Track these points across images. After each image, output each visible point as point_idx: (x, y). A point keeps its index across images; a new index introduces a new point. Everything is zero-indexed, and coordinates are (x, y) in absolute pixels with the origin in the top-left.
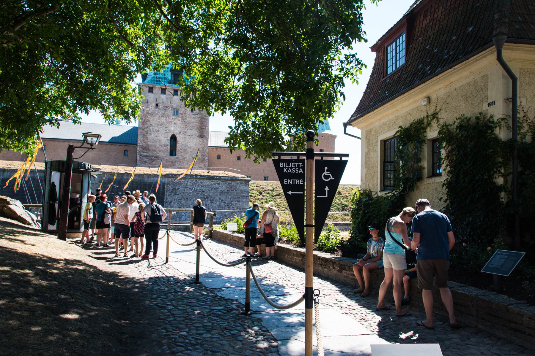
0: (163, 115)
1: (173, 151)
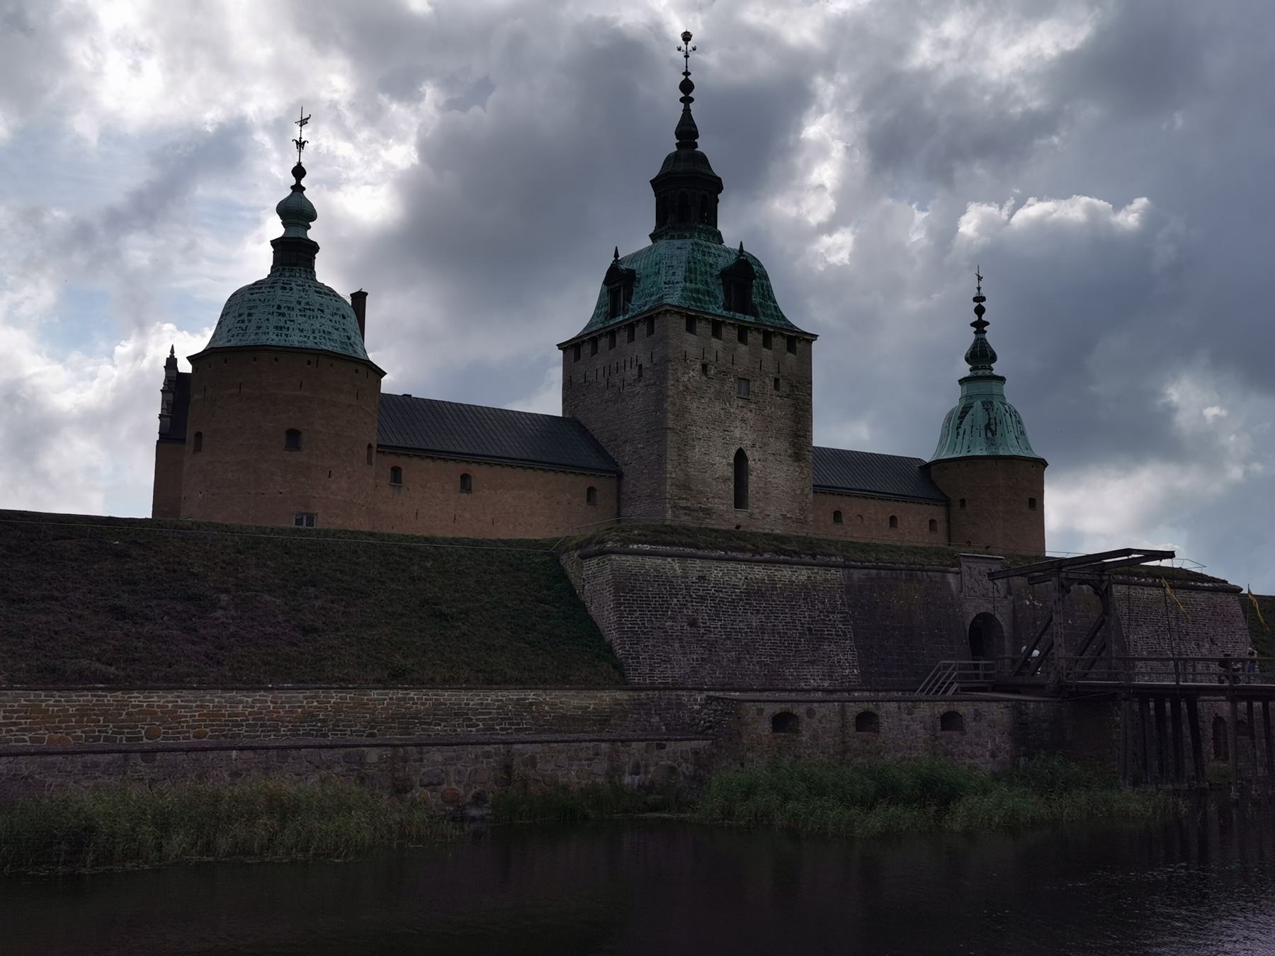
0: (719, 395)
1: (740, 499)
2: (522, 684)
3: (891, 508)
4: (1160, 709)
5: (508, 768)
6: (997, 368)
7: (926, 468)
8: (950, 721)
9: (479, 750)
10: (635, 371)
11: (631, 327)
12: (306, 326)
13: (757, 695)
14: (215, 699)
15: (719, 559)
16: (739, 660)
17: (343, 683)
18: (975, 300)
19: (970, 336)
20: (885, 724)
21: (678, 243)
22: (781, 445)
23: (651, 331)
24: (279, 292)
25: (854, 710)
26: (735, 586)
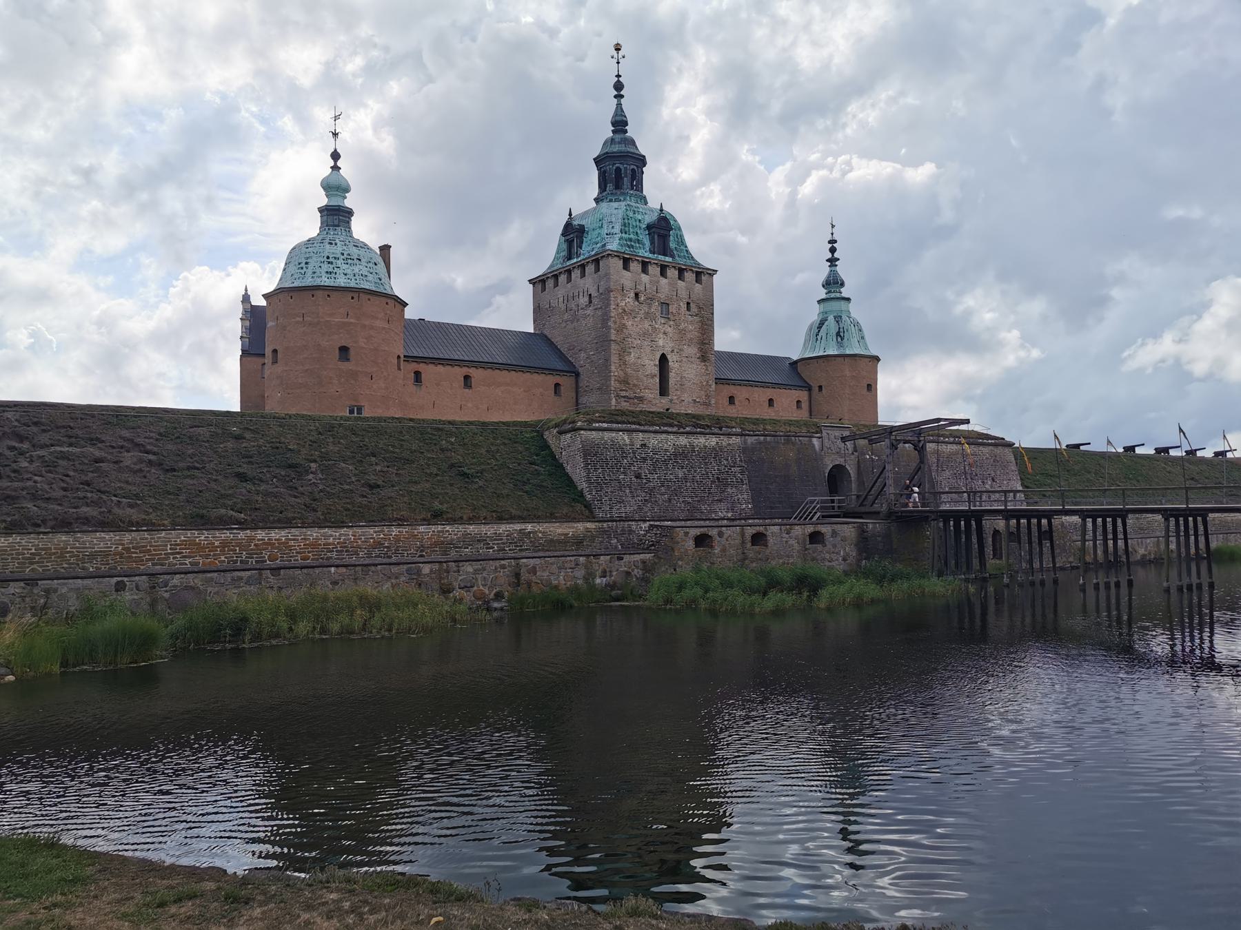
1: (664, 391)
2: (523, 519)
3: (770, 393)
4: (957, 525)
5: (517, 575)
6: (845, 292)
7: (794, 364)
8: (815, 537)
9: (497, 563)
10: (587, 299)
11: (583, 267)
12: (348, 271)
13: (683, 523)
14: (314, 534)
15: (655, 432)
16: (670, 500)
17: (400, 522)
18: (830, 242)
19: (825, 270)
20: (771, 540)
21: (615, 205)
22: (692, 351)
23: (597, 270)
24: (328, 246)
25: (750, 531)
26: (666, 450)
